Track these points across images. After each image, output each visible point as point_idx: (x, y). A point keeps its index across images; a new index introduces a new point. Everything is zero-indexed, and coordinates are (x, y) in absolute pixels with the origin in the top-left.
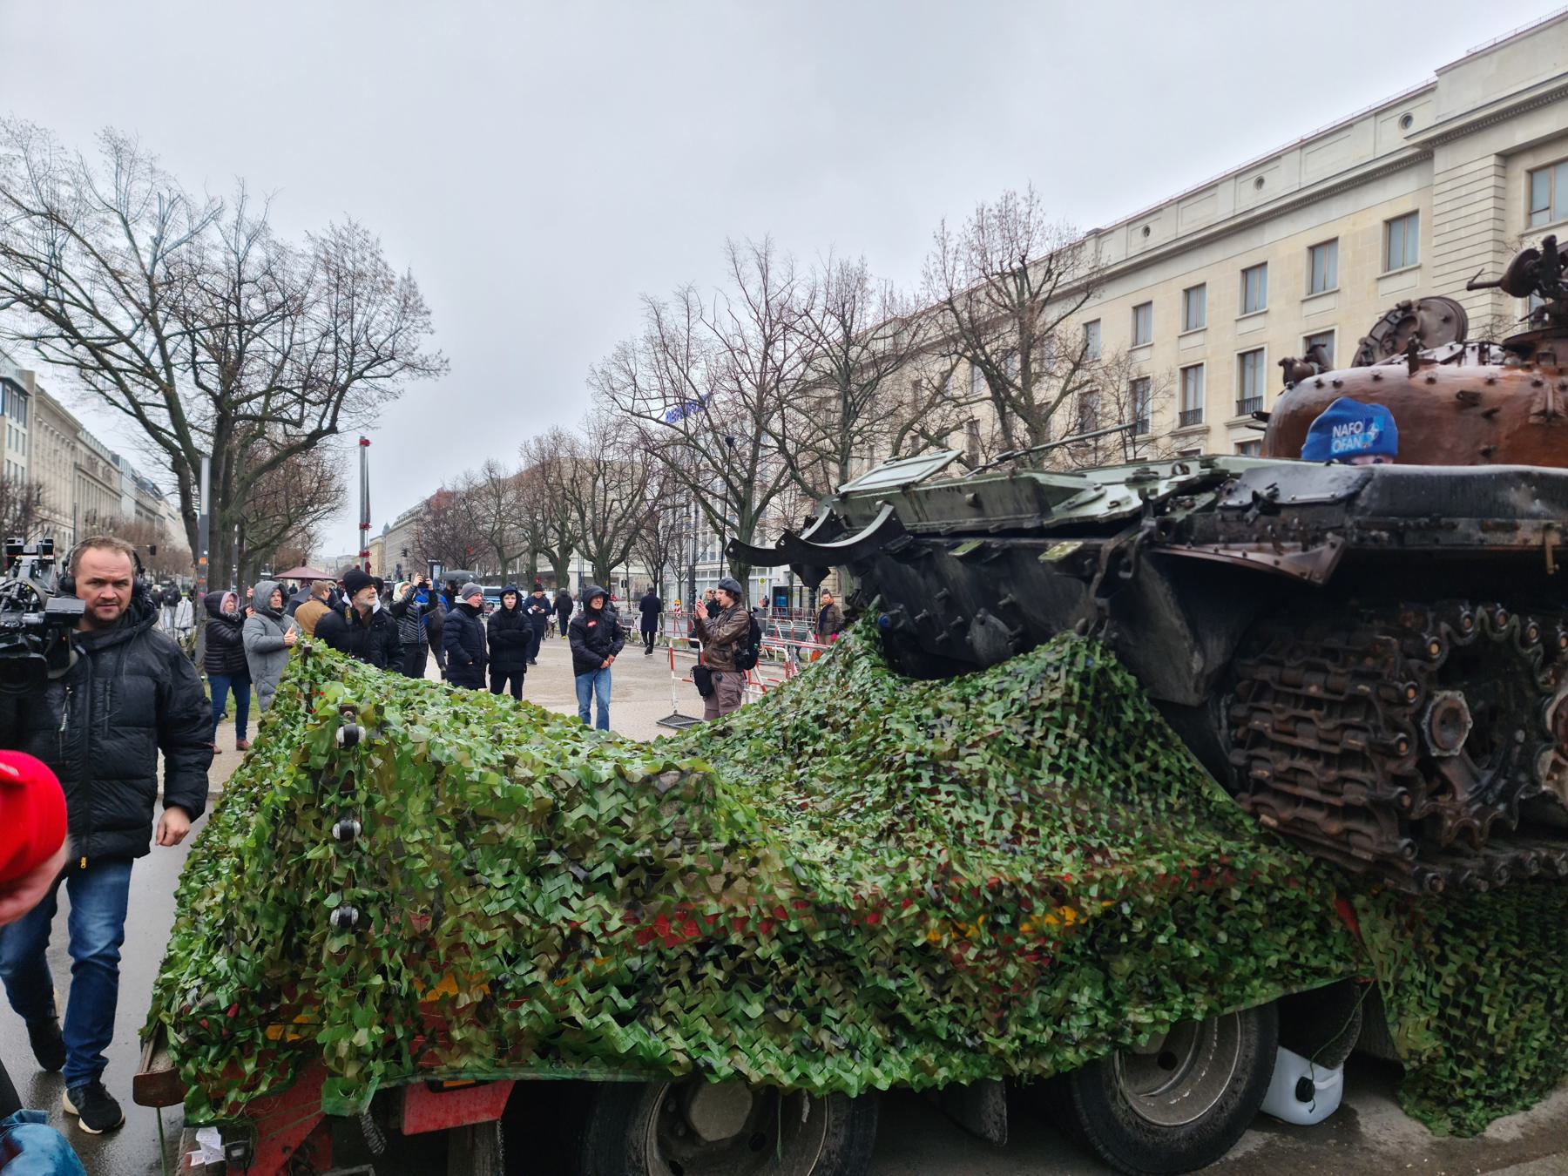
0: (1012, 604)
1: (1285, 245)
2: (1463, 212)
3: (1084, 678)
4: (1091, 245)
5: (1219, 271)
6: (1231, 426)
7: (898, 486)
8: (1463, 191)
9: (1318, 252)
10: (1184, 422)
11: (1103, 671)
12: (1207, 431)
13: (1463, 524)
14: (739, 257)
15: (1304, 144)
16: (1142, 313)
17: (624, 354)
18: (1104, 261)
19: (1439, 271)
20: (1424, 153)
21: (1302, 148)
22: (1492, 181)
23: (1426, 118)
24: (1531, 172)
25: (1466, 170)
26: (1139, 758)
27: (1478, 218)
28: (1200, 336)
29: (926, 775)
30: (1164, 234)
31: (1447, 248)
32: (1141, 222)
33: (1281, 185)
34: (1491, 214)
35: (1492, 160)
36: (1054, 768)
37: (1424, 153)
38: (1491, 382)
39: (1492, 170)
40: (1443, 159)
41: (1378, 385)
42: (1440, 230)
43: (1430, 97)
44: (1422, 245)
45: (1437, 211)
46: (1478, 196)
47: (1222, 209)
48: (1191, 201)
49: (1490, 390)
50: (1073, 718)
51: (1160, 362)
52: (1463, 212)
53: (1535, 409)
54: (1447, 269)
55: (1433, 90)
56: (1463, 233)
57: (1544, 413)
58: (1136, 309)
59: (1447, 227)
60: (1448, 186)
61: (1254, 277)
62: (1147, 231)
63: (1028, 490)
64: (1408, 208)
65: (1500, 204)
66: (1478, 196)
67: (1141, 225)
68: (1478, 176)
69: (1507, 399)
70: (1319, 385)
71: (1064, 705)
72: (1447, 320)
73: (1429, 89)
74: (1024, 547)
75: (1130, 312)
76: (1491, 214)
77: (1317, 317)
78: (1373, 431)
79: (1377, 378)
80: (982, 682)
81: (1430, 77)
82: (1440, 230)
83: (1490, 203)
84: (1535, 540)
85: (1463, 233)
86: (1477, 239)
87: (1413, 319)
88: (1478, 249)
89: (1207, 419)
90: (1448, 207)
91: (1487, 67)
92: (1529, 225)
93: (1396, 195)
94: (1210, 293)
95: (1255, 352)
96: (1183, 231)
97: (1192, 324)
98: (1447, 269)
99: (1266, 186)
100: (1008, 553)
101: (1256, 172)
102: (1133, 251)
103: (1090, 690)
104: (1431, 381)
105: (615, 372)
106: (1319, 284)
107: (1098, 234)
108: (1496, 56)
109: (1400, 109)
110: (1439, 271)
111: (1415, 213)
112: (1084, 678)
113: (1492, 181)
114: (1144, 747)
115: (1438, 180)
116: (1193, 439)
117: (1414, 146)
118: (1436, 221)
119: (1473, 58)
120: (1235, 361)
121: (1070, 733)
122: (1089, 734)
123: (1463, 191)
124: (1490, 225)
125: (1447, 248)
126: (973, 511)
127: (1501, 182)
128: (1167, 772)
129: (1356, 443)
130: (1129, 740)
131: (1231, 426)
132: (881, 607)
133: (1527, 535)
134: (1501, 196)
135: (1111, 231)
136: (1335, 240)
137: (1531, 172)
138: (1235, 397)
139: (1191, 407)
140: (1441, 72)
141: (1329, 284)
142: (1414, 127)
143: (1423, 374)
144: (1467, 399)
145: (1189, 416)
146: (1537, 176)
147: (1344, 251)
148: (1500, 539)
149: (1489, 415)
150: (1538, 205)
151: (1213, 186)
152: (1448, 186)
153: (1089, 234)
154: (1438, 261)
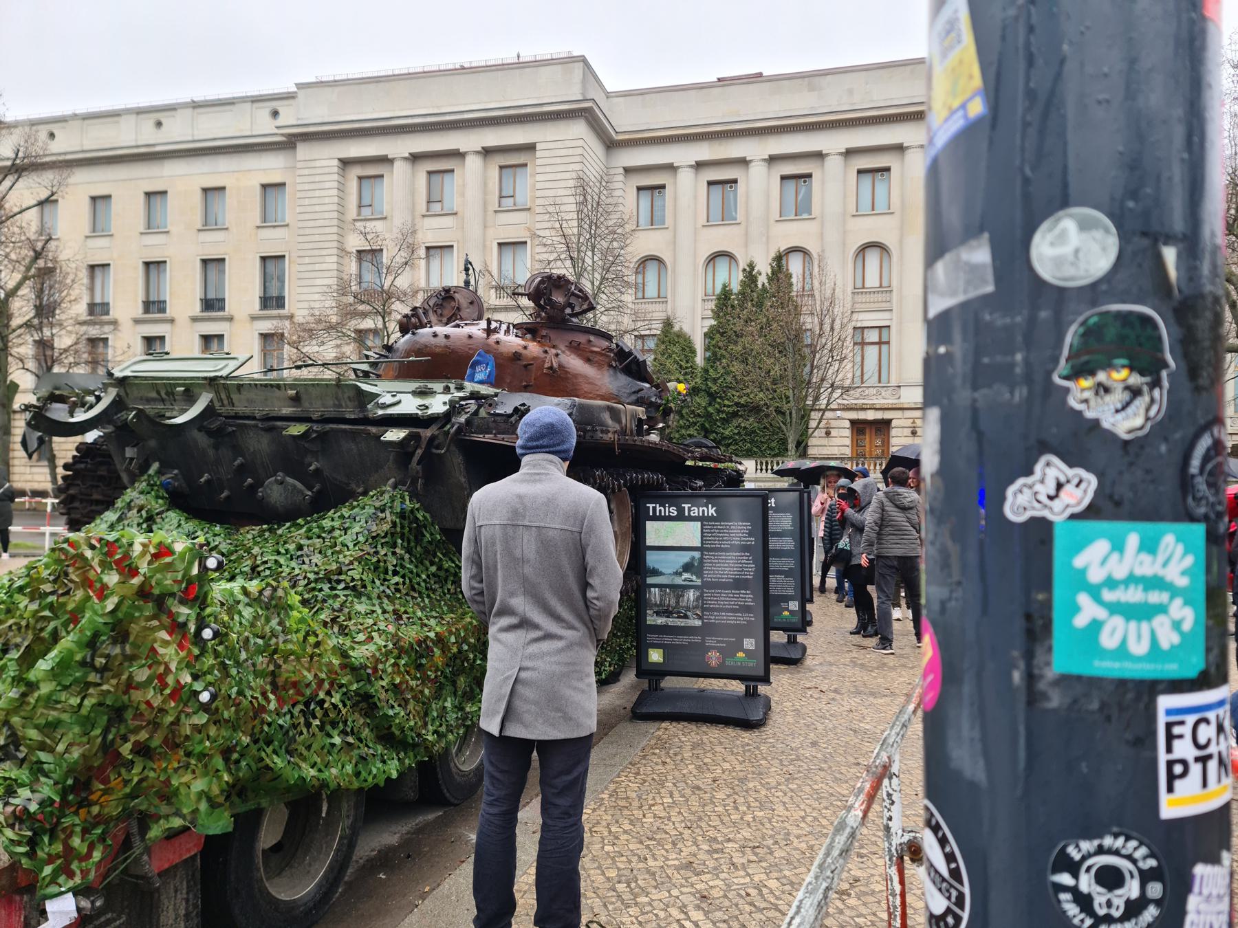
0: (317, 470)
2: (317, 193)
3: (402, 515)
7: (205, 378)
8: (317, 178)
9: (209, 193)
11: (412, 511)
15: (195, 105)
19: (302, 232)
20: (290, 143)
21: (194, 107)
22: (336, 177)
23: (290, 117)
24: (360, 178)
25: (318, 164)
26: (432, 564)
27: (327, 200)
28: (108, 239)
29: (326, 587)
31: (307, 217)
33: (177, 132)
35: (336, 162)
36: (395, 573)
37: (290, 143)
38: (525, 348)
40: (304, 151)
41: (470, 342)
43: (291, 102)
45: (299, 187)
46: (327, 185)
47: (127, 136)
49: (524, 352)
50: (399, 541)
52: (317, 193)
53: (546, 365)
54: (307, 231)
55: (293, 98)
57: (551, 368)
59: (307, 202)
60: (307, 172)
63: (352, 393)
66: (327, 185)
68: (326, 170)
69: (534, 358)
70: (435, 335)
71: (393, 535)
72: (471, 303)
73: (289, 97)
74: (344, 431)
76: (336, 200)
77: (213, 245)
79: (470, 337)
80: (327, 523)
83: (335, 192)
85: (317, 208)
86: (327, 215)
87: (453, 299)
88: (327, 223)
89: (114, 313)
90: (307, 187)
92: (359, 214)
93: (271, 167)
94: (116, 205)
95: (158, 263)
97: (99, 226)
98: (307, 231)
99: (164, 128)
100: (323, 436)
101: (158, 114)
103: (406, 523)
104: (498, 343)
106: (211, 220)
108: (337, 90)
109: (273, 102)
110: (302, 232)
111: (283, 184)
112: (402, 515)
114: (435, 555)
115: (299, 165)
116: (107, 328)
117: (282, 135)
118: (299, 195)
121: (398, 550)
122: (409, 551)
123: (317, 178)
124: (335, 207)
125: (307, 217)
126: (291, 403)
127: (341, 179)
128: (447, 571)
130: (427, 551)
131: (137, 321)
132: (160, 472)
134: (341, 189)
136: (224, 188)
137: (360, 178)
138: (141, 297)
141: (220, 220)
142: (281, 121)
143: (494, 337)
145: (98, 310)
147: (230, 198)
149: (526, 366)
150: (366, 201)
151: (115, 114)
152: (307, 172)
154: (301, 224)
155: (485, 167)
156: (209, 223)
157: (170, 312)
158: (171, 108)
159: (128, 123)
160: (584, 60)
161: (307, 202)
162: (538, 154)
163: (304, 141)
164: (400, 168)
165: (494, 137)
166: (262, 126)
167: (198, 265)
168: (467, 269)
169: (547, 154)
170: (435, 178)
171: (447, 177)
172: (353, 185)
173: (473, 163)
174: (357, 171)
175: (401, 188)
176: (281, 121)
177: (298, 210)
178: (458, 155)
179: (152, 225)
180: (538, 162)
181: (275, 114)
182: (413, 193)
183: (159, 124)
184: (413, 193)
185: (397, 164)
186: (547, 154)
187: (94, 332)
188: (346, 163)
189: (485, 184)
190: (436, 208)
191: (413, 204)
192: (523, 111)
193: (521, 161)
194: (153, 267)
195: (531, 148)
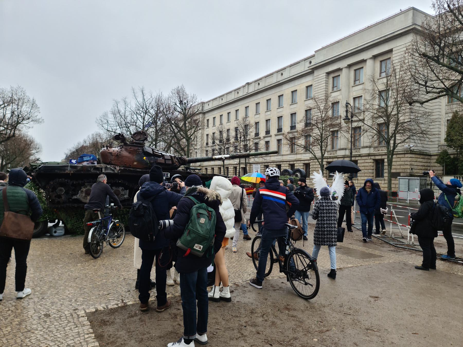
1: (287, 90)
2: (319, 86)
4: (247, 86)
5: (273, 95)
6: (276, 135)
8: (320, 81)
9: (294, 93)
10: (266, 134)
12: (271, 136)
13: (56, 171)
14: (135, 91)
15: (291, 66)
17: (105, 115)
18: (249, 92)
22: (325, 79)
23: (315, 62)
24: (333, 78)
25: (320, 76)
27: (322, 88)
30: (263, 85)
32: (257, 81)
33: (287, 75)
34: (325, 87)
35: (325, 74)
39: (325, 77)
40: (316, 73)
42: (315, 90)
44: (313, 93)
46: (323, 82)
51: (252, 120)
52: (319, 86)
56: (319, 91)
59: (317, 90)
60: (317, 80)
61: (281, 98)
62: (259, 84)
64: (310, 84)
65: (327, 85)
66: (323, 82)
67: (257, 82)
73: (313, 56)
75: (255, 105)
76: (325, 87)
77: (294, 108)
78: (91, 157)
81: (313, 53)
82: (315, 90)
83: (324, 84)
85: (319, 91)
86: (322, 93)
90: (317, 85)
91: (324, 51)
92: (333, 90)
93: (307, 81)
96: (266, 85)
101: (281, 71)
102: (256, 89)
105: (103, 119)
106: (294, 101)
107: (248, 84)
111: (312, 85)
113: (325, 79)
115: (315, 78)
118: (315, 88)
119: (323, 48)
120: (277, 119)
123: (320, 81)
124: (324, 90)
127: (327, 79)
129: (89, 159)
131: (276, 135)
133: (66, 172)
134: (327, 83)
135: (251, 83)
136: (296, 90)
137: (333, 78)
138: (277, 128)
140: (316, 52)
142: (312, 64)
144: (111, 153)
146: (335, 79)
150: (335, 86)
152: (317, 80)
153: (246, 84)
155: (374, 63)
156: (293, 102)
157: (283, 132)
158: (284, 69)
159: (275, 75)
160: (414, 9)
161: (317, 90)
162: (394, 53)
163: (316, 69)
164: (344, 71)
165: (376, 51)
166: (305, 67)
167: (290, 116)
168: (347, 106)
169: (397, 52)
170: (358, 72)
171: (361, 70)
172: (331, 80)
173: (370, 63)
174: (332, 75)
175: (346, 77)
176: (312, 64)
177: (315, 93)
178: (364, 61)
179: (280, 106)
180: (394, 56)
181: (310, 62)
182: (349, 79)
183: (282, 74)
184: (349, 79)
185: (344, 70)
186: (397, 52)
187: (256, 141)
188: (328, 74)
189: (374, 69)
190: (357, 83)
191: (349, 83)
192: (387, 37)
193: (389, 57)
194: (280, 118)
195: (391, 51)
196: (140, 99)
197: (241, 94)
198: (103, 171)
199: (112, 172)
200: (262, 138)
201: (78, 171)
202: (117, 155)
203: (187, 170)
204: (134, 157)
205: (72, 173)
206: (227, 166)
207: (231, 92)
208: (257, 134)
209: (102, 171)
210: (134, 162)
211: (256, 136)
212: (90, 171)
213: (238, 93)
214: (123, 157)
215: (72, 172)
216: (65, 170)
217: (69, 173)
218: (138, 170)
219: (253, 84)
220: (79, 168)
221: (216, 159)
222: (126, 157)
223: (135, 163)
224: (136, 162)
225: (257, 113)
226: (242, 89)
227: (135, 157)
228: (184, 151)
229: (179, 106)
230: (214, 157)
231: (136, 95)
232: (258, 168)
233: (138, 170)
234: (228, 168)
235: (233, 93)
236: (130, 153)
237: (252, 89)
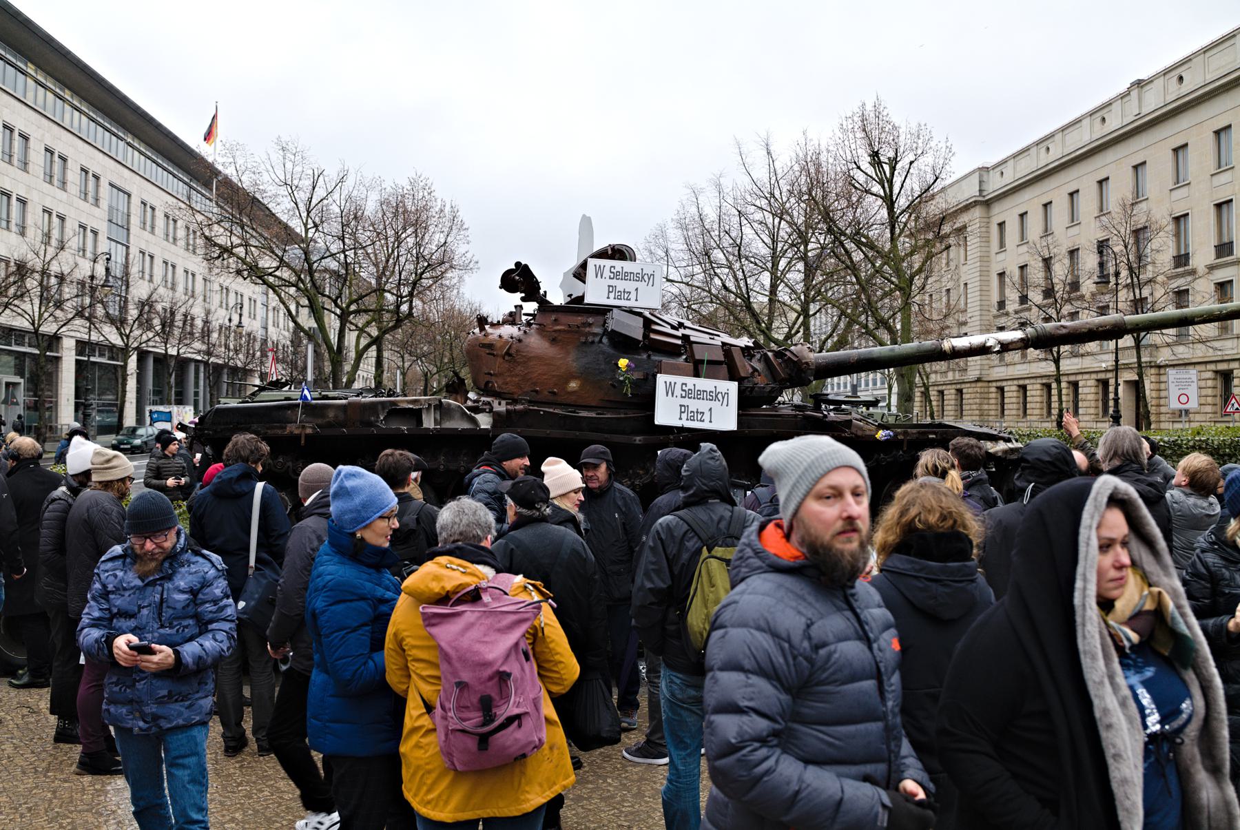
4: (1134, 93)
10: (1219, 256)
14: (744, 150)
16: (1181, 153)
17: (662, 233)
18: (1145, 111)
32: (1175, 71)
48: (1215, 51)
58: (1176, 150)
62: (1181, 78)
84: (297, 432)
96: (1209, 78)
97: (1223, 163)
102: (1170, 98)
107: (1139, 84)
133: (292, 429)
135: (1150, 81)
139: (1226, 240)
144: (490, 346)
148: (279, 432)
153: (1133, 85)
187: (1180, 283)
196: (761, 174)
197: (1116, 122)
198: (429, 422)
199: (466, 425)
200: (1201, 270)
201: (330, 425)
202: (508, 353)
203: (817, 408)
204: (570, 358)
205: (307, 436)
206: (1072, 378)
207: (1077, 122)
208: (1182, 259)
209: (420, 422)
210: (567, 382)
211: (1177, 265)
212: (371, 424)
213: (1104, 119)
214: (529, 359)
215: (309, 431)
216: (285, 421)
217: (298, 437)
218: (584, 414)
219: (1159, 83)
220: (331, 414)
221: (957, 354)
222: (539, 358)
223: (573, 385)
224: (572, 377)
225: (1179, 181)
226: (1116, 106)
227: (571, 360)
228: (891, 330)
229: (871, 171)
230: (946, 345)
231: (748, 161)
232: (1189, 382)
233: (584, 414)
234: (1075, 385)
235: (1086, 122)
236: (553, 341)
237: (1153, 102)
